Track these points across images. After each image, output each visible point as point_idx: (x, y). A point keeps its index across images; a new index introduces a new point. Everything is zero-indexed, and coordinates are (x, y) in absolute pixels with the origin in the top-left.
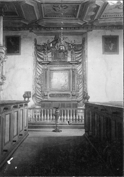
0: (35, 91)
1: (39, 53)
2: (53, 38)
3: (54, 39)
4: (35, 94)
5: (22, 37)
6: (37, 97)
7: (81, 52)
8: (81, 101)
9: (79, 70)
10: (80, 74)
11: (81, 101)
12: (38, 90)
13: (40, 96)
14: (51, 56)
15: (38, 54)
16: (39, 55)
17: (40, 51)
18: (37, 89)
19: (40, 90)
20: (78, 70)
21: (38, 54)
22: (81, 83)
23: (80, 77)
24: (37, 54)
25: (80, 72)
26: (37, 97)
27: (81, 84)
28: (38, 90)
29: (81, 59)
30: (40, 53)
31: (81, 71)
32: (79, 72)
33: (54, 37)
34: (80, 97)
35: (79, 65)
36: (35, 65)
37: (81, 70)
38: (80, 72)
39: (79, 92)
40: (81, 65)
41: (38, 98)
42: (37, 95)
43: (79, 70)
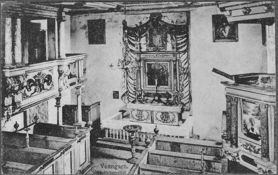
0: (127, 88)
2: (147, 18)
3: (149, 18)
4: (126, 92)
5: (106, 21)
6: (130, 94)
8: (187, 103)
9: (184, 60)
10: (184, 67)
11: (187, 103)
13: (133, 94)
14: (145, 42)
15: (129, 38)
19: (134, 86)
23: (185, 71)
26: (130, 94)
27: (186, 80)
29: (186, 46)
31: (186, 63)
32: (183, 64)
33: (148, 16)
34: (186, 97)
35: (184, 54)
37: (186, 61)
40: (187, 53)
41: (132, 97)
42: (130, 92)
43: (184, 60)
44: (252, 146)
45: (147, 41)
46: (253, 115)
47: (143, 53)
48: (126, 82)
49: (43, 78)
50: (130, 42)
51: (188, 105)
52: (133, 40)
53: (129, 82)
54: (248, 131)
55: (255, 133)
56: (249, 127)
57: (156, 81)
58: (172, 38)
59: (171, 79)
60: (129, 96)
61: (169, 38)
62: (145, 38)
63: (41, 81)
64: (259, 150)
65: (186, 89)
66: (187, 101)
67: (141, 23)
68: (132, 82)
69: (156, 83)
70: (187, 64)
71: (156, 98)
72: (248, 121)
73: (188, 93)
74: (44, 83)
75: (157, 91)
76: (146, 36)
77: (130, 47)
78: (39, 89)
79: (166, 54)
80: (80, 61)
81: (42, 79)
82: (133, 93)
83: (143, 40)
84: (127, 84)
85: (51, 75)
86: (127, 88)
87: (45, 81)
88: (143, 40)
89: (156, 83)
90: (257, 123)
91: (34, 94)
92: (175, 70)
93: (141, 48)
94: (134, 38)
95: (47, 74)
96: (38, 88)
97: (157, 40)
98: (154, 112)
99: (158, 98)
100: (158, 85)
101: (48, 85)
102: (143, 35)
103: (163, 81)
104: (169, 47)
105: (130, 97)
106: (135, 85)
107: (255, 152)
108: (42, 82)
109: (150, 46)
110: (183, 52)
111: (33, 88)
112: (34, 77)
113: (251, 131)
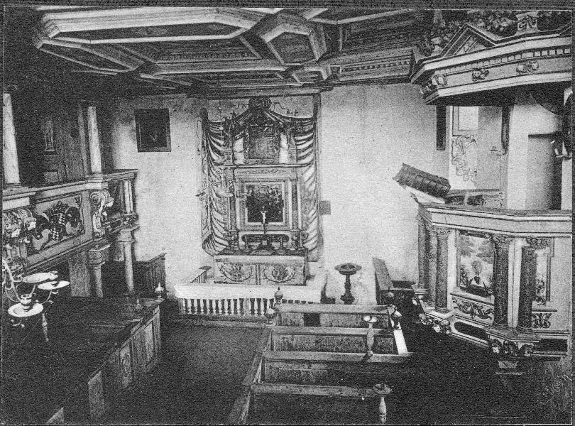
0: (212, 228)
1: (213, 140)
4: (210, 237)
7: (312, 137)
9: (309, 179)
12: (217, 225)
13: (222, 239)
16: (215, 145)
17: (216, 137)
18: (214, 220)
19: (223, 225)
20: (306, 180)
21: (215, 145)
22: (313, 209)
24: (211, 143)
25: (311, 185)
28: (219, 227)
30: (218, 141)
31: (313, 182)
35: (308, 169)
36: (206, 171)
37: (312, 180)
38: (311, 185)
39: (307, 232)
40: (313, 166)
41: (220, 244)
44: (475, 306)
45: (245, 148)
46: (479, 256)
47: (238, 167)
48: (209, 220)
49: (64, 213)
50: (214, 148)
51: (314, 253)
52: (219, 145)
53: (215, 219)
54: (468, 283)
55: (482, 286)
56: (471, 276)
57: (264, 214)
58: (289, 141)
59: (288, 210)
60: (216, 242)
61: (284, 143)
62: (241, 141)
63: (60, 220)
64: (489, 311)
65: (313, 226)
66: (314, 246)
67: (234, 114)
68: (220, 217)
69: (264, 218)
70: (314, 185)
71: (265, 243)
72: (469, 267)
73: (315, 233)
74: (66, 223)
75: (265, 231)
76: (244, 136)
77: (214, 156)
78: (56, 234)
79: (279, 169)
80: (126, 183)
81: (61, 215)
82: (222, 236)
83: (239, 145)
84: (211, 221)
85: (77, 206)
86: (212, 228)
87: (67, 219)
88: (239, 145)
89: (264, 218)
90: (487, 269)
91: (49, 244)
92: (295, 195)
93: (234, 159)
94: (222, 142)
95: (70, 206)
96: (55, 232)
97: (264, 145)
98: (261, 267)
99: (267, 244)
100: (267, 221)
101: (74, 225)
102: (238, 136)
103: (275, 212)
104: (284, 157)
105: (217, 244)
106: (225, 224)
107: (481, 316)
108: (62, 222)
109: (250, 158)
110: (307, 164)
111: (46, 233)
112: (46, 213)
113: (474, 283)
